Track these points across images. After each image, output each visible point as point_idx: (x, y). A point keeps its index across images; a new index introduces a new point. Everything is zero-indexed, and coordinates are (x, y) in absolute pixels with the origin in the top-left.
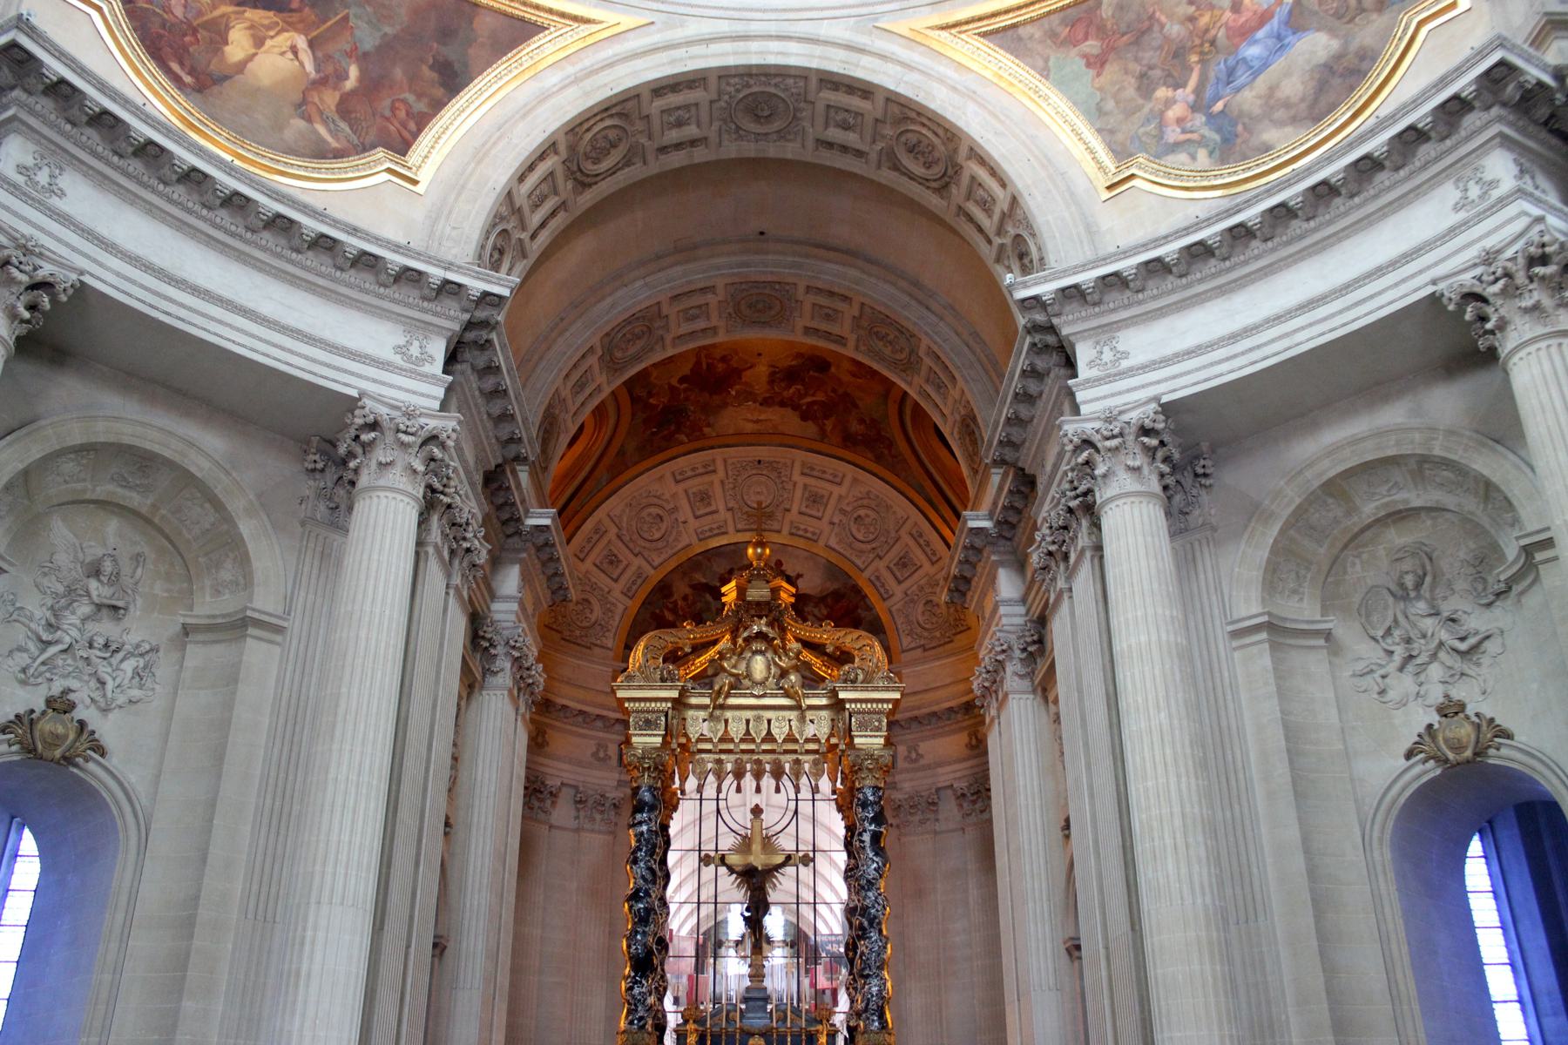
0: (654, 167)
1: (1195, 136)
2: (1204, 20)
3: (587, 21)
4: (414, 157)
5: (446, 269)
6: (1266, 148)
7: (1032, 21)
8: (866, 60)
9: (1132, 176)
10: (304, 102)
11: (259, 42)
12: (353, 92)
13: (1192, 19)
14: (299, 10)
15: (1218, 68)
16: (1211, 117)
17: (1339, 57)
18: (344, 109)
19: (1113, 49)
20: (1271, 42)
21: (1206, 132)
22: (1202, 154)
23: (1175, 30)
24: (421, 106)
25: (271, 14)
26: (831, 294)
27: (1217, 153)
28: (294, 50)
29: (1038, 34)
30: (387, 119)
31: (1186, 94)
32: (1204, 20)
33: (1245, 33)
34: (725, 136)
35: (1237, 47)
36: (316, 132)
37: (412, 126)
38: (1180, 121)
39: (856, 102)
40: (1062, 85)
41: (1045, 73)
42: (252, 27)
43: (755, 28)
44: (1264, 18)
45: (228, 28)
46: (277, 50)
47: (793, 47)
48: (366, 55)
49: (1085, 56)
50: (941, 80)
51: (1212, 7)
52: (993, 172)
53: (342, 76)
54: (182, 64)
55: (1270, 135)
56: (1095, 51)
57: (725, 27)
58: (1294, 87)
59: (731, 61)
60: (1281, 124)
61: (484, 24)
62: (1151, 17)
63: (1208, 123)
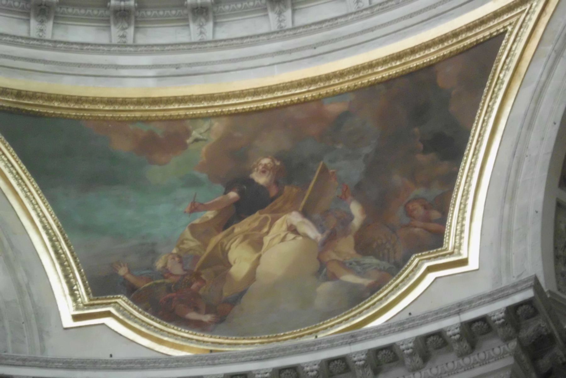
4: (450, 242)
5: (459, 313)
10: (322, 265)
12: (365, 225)
18: (363, 246)
24: (436, 190)
25: (257, 214)
28: (293, 229)
30: (407, 226)
36: (346, 284)
37: (435, 214)
42: (246, 237)
45: (225, 253)
46: (277, 240)
48: (359, 186)
54: (197, 309)
61: (446, 79)
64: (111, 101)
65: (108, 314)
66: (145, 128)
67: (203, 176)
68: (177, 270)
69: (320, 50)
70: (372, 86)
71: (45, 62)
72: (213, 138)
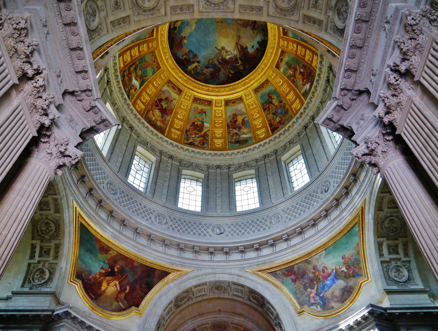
0: (194, 301)
1: (317, 302)
2: (317, 274)
3: (180, 271)
6: (333, 308)
7: (279, 270)
8: (242, 279)
9: (304, 311)
10: (117, 297)
11: (108, 284)
12: (128, 293)
13: (314, 273)
14: (117, 275)
15: (321, 285)
16: (320, 297)
17: (346, 287)
18: (125, 298)
19: (298, 278)
20: (331, 281)
21: (319, 301)
22: (319, 307)
23: (311, 275)
24: (142, 294)
26: (237, 325)
27: (322, 307)
28: (116, 285)
29: (281, 273)
31: (314, 291)
32: (317, 274)
33: (326, 278)
34: (211, 293)
35: (324, 281)
36: (120, 305)
37: (140, 299)
38: (314, 297)
39: (240, 288)
40: (286, 286)
41: (283, 283)
43: (217, 271)
44: (330, 275)
45: (102, 282)
47: (226, 276)
48: (131, 283)
49: (291, 279)
50: (259, 284)
51: (318, 271)
52: (273, 307)
53: (126, 290)
55: (333, 304)
56: (294, 278)
57: (210, 271)
58: (337, 293)
59: (212, 279)
60: (335, 302)
61: (157, 273)
62: (305, 271)
63: (320, 299)
64: (102, 236)
65: (77, 284)
66: (103, 245)
67: (107, 262)
68: (93, 281)
69: (140, 250)
70: (144, 265)
71: (96, 219)
72: (113, 255)
